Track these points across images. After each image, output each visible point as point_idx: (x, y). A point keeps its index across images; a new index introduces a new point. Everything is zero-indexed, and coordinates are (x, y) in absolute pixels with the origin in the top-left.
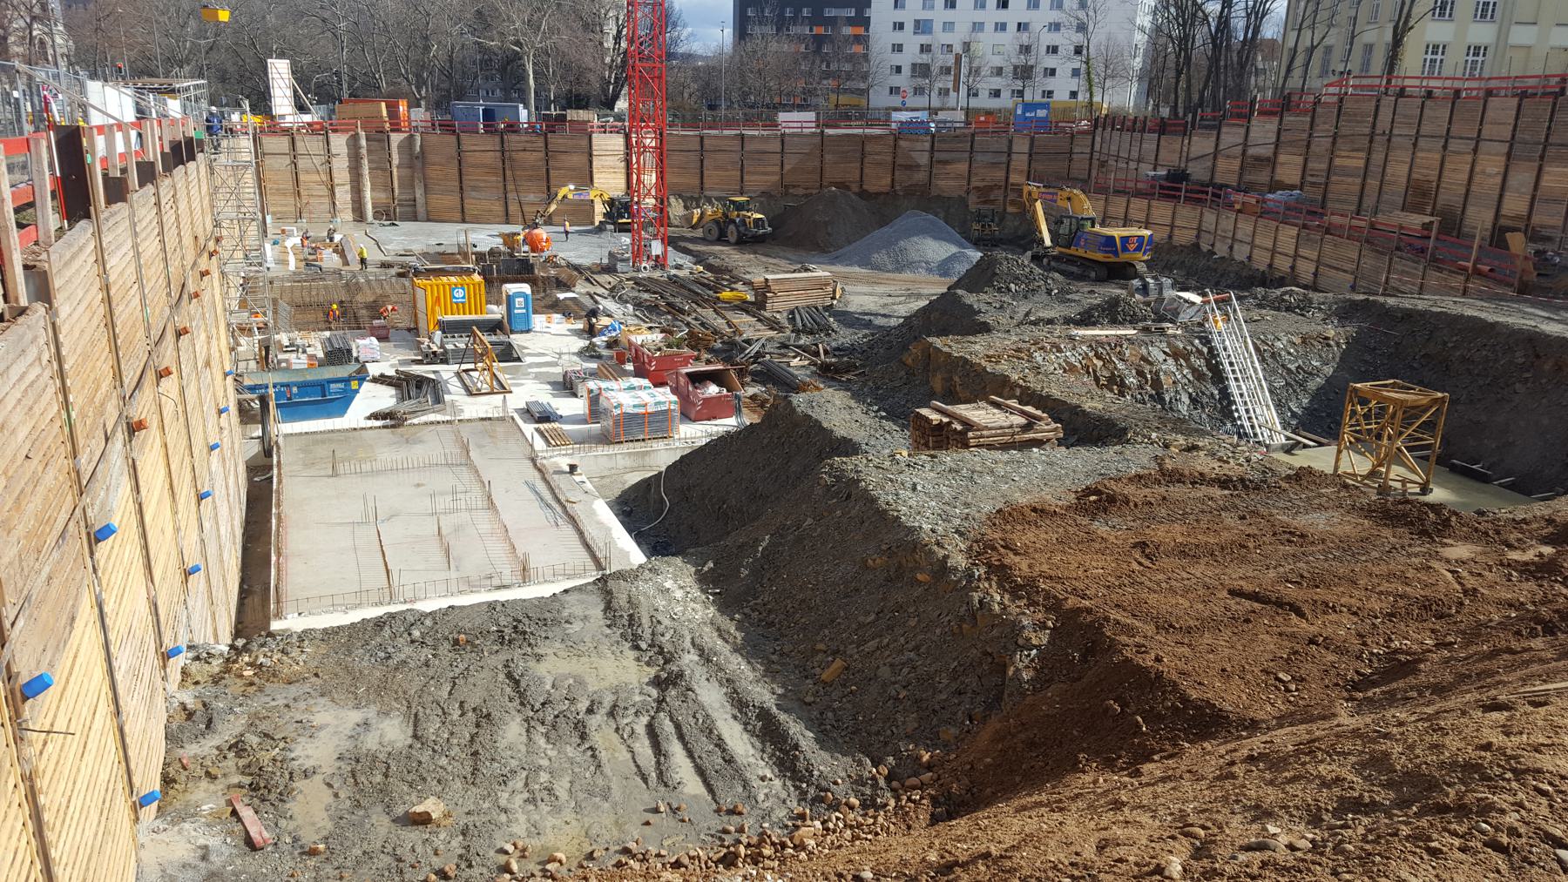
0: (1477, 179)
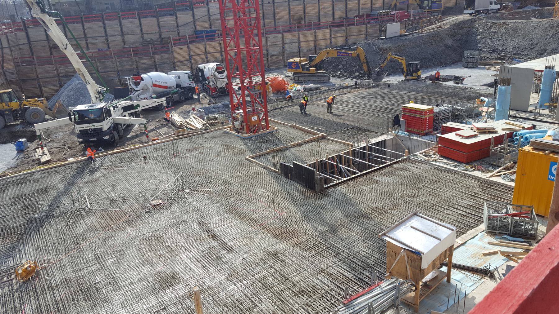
0: (321, 10)
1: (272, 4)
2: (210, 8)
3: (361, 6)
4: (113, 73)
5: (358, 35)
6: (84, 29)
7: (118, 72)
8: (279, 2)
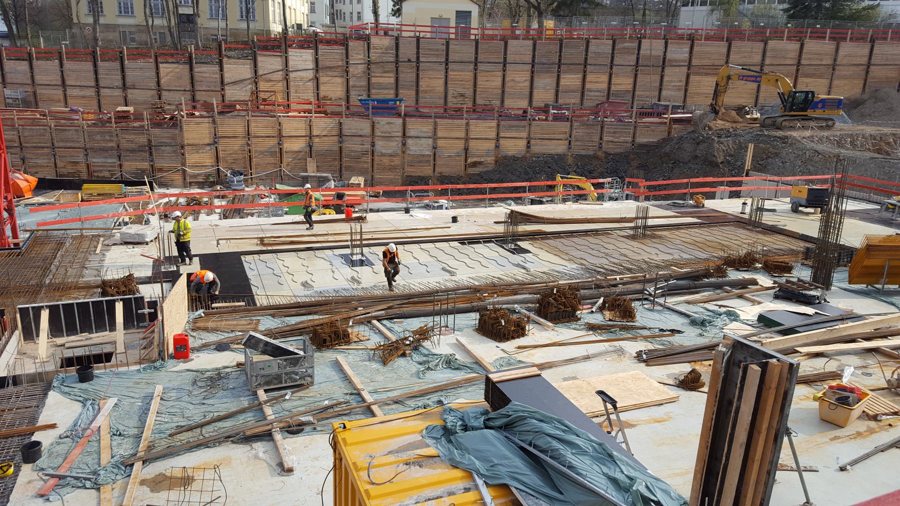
0: (507, 85)
1: (415, 64)
2: (290, 57)
3: (588, 86)
4: (77, 152)
5: (554, 139)
6: (62, 71)
7: (86, 150)
8: (428, 62)
